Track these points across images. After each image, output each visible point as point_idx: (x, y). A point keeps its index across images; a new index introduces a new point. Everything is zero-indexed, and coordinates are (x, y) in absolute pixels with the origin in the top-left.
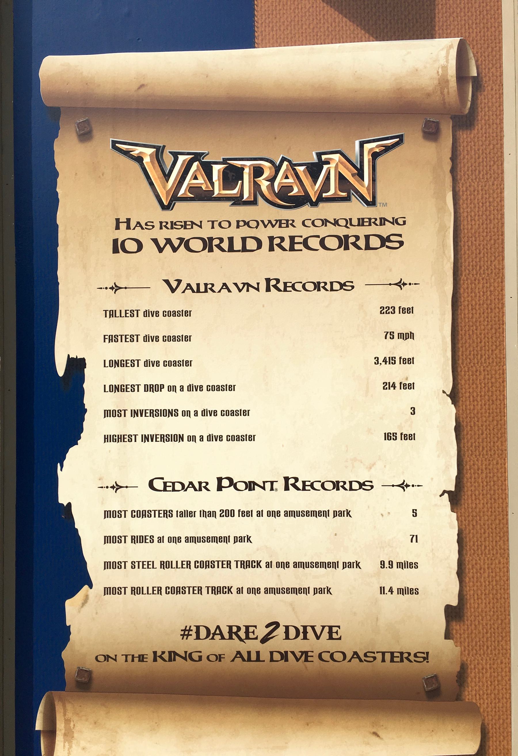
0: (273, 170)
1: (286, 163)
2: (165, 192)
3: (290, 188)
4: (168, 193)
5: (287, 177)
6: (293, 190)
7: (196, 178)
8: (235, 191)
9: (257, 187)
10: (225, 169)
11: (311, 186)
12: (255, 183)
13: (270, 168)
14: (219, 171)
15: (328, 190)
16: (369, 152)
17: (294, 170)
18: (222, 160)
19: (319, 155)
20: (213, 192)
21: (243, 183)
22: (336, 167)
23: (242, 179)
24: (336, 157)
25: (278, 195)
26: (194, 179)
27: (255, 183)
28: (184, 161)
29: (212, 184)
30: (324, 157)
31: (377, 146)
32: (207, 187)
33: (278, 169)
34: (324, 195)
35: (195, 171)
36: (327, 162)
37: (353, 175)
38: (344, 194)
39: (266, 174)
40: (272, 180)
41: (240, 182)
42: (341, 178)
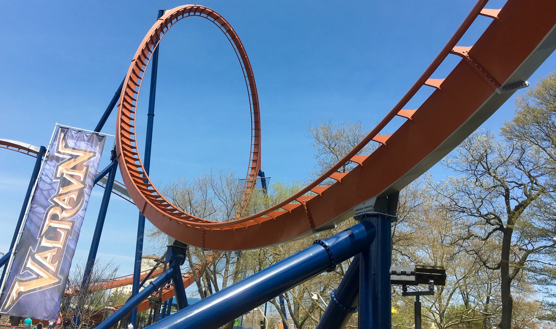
0: (57, 207)
1: (55, 199)
5: (64, 200)
8: (63, 234)
9: (63, 220)
10: (46, 237)
12: (62, 220)
14: (46, 242)
15: (80, 177)
17: (60, 195)
19: (56, 178)
20: (59, 248)
21: (59, 228)
22: (67, 170)
23: (56, 228)
24: (60, 168)
25: (74, 207)
27: (62, 220)
28: (31, 263)
29: (54, 248)
30: (58, 176)
32: (54, 251)
33: (57, 205)
34: (82, 180)
35: (41, 257)
36: (62, 174)
37: (74, 161)
38: (85, 168)
39: (58, 213)
40: (63, 209)
41: (58, 230)
42: (74, 168)
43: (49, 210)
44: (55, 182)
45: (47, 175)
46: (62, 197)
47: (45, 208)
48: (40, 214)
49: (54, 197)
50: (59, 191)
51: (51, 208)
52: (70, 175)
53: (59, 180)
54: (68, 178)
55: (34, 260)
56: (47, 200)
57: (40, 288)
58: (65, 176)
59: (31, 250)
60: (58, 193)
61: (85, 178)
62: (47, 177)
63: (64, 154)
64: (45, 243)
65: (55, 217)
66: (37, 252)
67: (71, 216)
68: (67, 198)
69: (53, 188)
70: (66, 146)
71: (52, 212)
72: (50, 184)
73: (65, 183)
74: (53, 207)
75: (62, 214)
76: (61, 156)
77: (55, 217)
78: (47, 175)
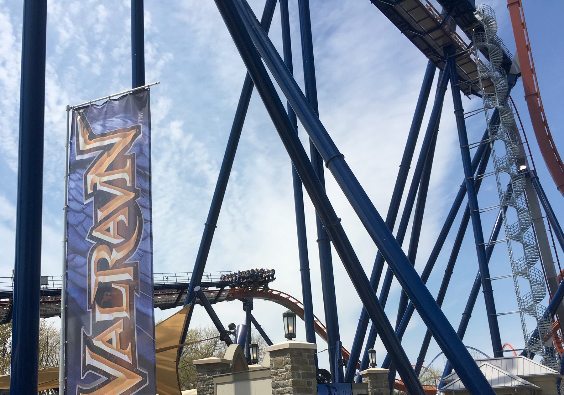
0: (101, 247)
1: (94, 234)
2: (128, 380)
3: (120, 224)
4: (129, 377)
5: (108, 230)
6: (122, 221)
7: (110, 342)
11: (118, 200)
12: (114, 267)
13: (99, 251)
14: (102, 313)
16: (89, 144)
17: (101, 222)
18: (91, 310)
19: (88, 196)
21: (114, 282)
24: (90, 177)
25: (128, 239)
26: (112, 344)
27: (114, 267)
30: (90, 191)
31: (84, 136)
32: (119, 327)
33: (100, 242)
34: (129, 184)
35: (103, 342)
36: (95, 186)
37: (109, 155)
40: (111, 247)
41: (113, 286)
42: (111, 168)
43: (91, 255)
44: (87, 205)
46: (104, 227)
48: (82, 267)
49: (92, 229)
50: (96, 217)
51: (93, 251)
53: (92, 199)
54: (105, 189)
55: (95, 350)
56: (84, 239)
60: (96, 221)
62: (75, 202)
63: (90, 151)
64: (101, 316)
65: (103, 265)
66: (96, 334)
67: (127, 256)
68: (111, 225)
70: (92, 137)
72: (82, 211)
73: (102, 199)
74: (95, 248)
75: (112, 257)
76: (86, 156)
77: (103, 265)
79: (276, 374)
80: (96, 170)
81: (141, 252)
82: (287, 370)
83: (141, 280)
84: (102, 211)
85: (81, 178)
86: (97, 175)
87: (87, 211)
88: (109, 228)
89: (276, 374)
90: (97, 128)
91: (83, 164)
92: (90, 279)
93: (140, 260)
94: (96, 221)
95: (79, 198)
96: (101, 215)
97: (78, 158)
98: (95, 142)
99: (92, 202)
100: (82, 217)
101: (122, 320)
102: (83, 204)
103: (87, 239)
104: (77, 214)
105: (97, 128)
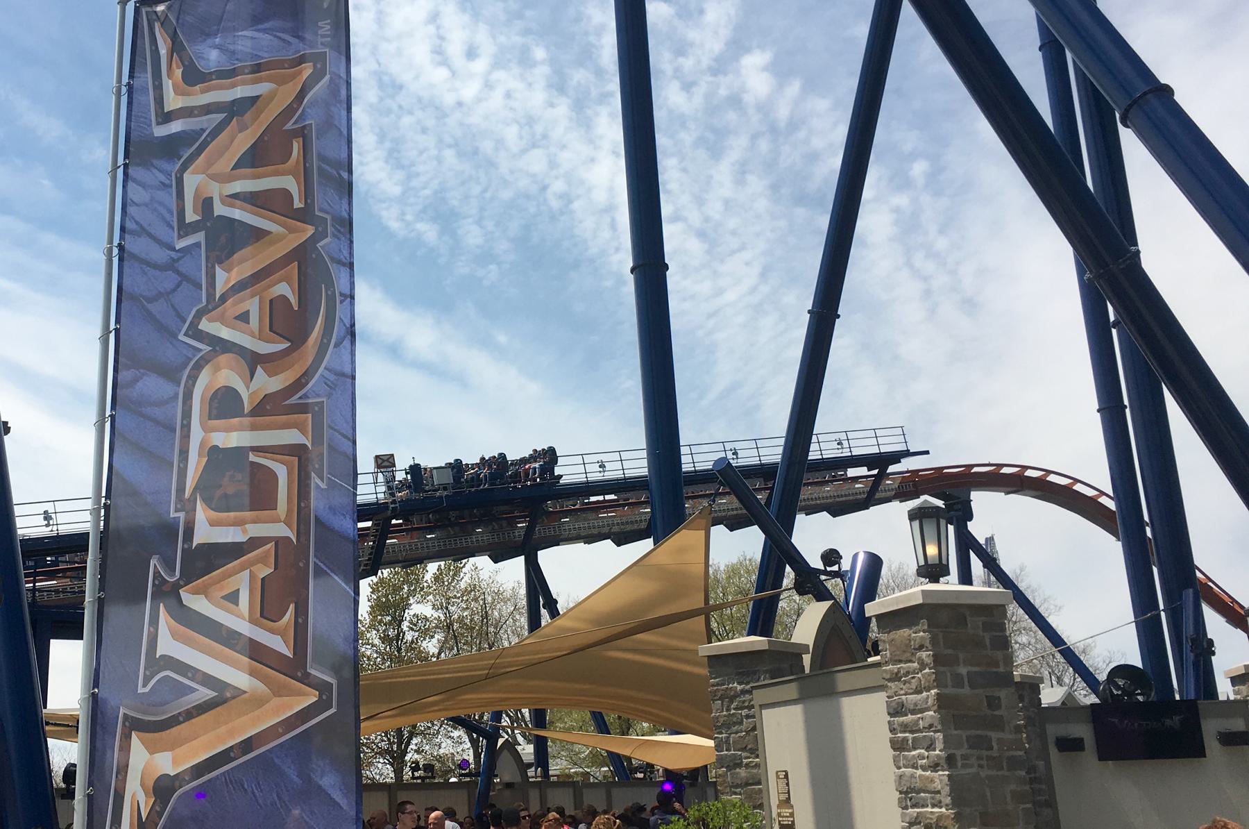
0: (223, 359)
1: (205, 325)
5: (244, 317)
6: (283, 298)
10: (208, 502)
11: (272, 243)
13: (217, 369)
15: (286, 194)
17: (224, 298)
18: (182, 515)
19: (185, 229)
24: (192, 181)
28: (175, 635)
30: (191, 217)
32: (263, 560)
36: (207, 204)
43: (193, 378)
45: (143, 231)
46: (232, 308)
47: (170, 373)
49: (199, 315)
51: (198, 367)
52: (235, 196)
53: (200, 237)
56: (175, 336)
57: (247, 745)
58: (219, 209)
59: (157, 574)
60: (210, 295)
61: (307, 193)
69: (184, 278)
71: (204, 384)
72: (171, 266)
75: (255, 385)
78: (143, 231)
79: (896, 677)
80: (210, 164)
81: (332, 377)
82: (923, 665)
83: (329, 446)
84: (228, 270)
85: (167, 182)
86: (213, 177)
87: (185, 266)
88: (248, 311)
89: (896, 677)
90: (211, 57)
91: (171, 147)
92: (186, 436)
93: (329, 396)
94: (210, 295)
95: (160, 231)
96: (224, 279)
97: (160, 131)
98: (203, 92)
99: (198, 245)
100: (167, 281)
101: (271, 546)
102: (173, 249)
103: (181, 337)
104: (151, 271)
105: (211, 57)
